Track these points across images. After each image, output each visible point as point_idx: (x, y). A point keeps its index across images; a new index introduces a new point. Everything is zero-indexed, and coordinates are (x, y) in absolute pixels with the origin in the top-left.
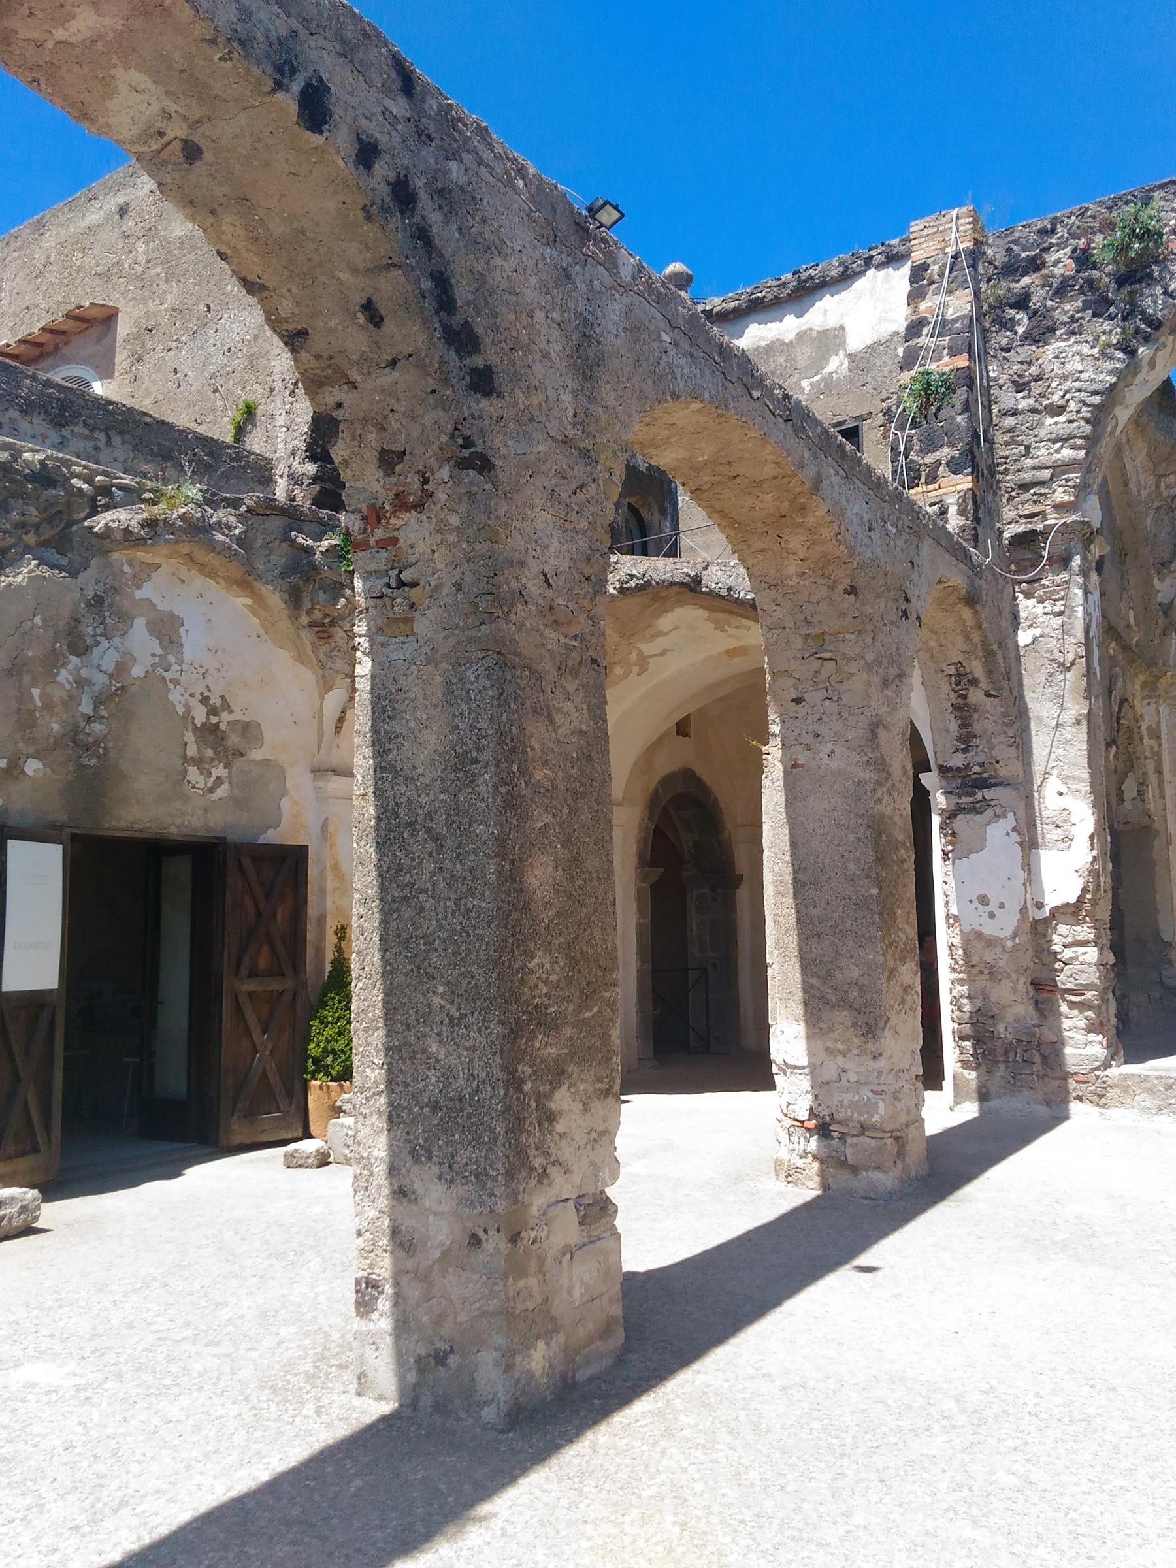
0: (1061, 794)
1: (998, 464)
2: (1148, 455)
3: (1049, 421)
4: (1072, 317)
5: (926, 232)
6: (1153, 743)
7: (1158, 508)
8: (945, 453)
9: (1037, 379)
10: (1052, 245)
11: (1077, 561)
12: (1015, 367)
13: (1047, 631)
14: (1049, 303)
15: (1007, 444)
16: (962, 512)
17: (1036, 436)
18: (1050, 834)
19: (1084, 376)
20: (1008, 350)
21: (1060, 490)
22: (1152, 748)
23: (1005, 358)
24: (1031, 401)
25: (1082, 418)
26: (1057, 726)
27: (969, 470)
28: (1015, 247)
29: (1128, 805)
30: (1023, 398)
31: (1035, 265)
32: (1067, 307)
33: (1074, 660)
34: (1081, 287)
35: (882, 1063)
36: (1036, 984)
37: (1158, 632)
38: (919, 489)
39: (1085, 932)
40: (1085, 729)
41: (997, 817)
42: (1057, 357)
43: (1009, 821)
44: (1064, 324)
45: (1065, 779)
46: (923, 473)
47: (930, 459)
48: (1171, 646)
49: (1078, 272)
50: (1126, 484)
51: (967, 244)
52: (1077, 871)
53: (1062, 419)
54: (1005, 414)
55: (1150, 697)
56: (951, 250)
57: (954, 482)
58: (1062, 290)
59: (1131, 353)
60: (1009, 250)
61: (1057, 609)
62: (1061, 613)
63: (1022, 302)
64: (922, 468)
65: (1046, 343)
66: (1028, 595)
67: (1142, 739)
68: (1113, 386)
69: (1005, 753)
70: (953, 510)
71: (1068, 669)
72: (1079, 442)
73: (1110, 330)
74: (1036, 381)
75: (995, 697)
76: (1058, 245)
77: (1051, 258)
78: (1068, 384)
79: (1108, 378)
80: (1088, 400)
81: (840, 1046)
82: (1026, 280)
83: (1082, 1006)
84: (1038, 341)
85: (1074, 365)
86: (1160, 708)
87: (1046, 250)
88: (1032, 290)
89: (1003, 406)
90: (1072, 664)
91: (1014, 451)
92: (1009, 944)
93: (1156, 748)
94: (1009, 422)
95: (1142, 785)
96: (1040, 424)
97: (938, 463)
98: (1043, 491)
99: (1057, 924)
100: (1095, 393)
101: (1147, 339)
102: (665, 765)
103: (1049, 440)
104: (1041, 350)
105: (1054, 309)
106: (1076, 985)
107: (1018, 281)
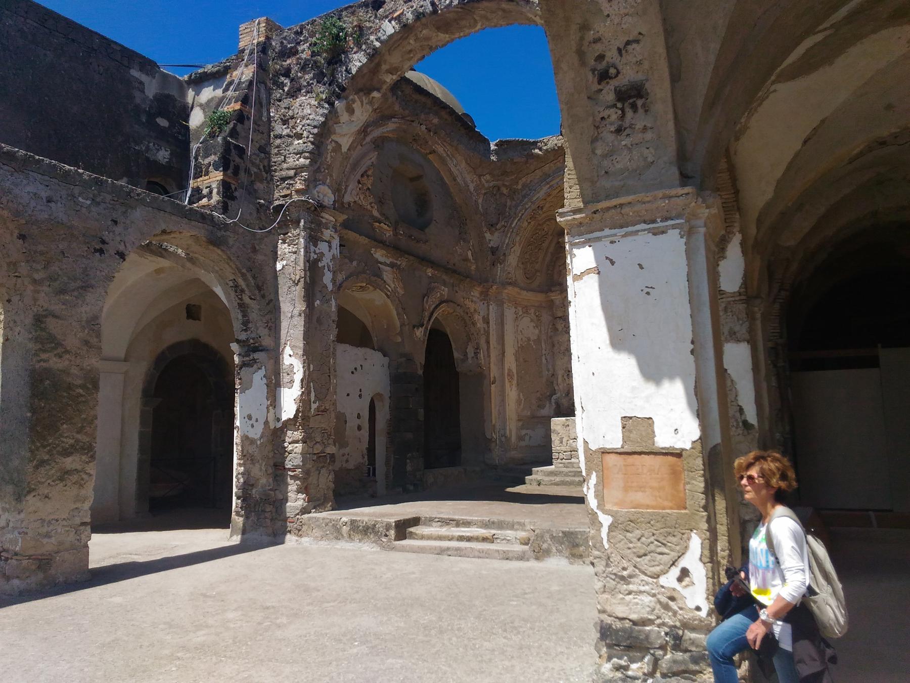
0: (290, 356)
1: (272, 166)
2: (466, 162)
3: (296, 142)
4: (308, 82)
5: (246, 31)
6: (485, 326)
7: (485, 194)
8: (213, 158)
9: (292, 118)
10: (301, 41)
11: (302, 223)
12: (282, 111)
13: (289, 262)
14: (299, 74)
15: (276, 154)
16: (218, 193)
17: (288, 151)
18: (285, 379)
19: (311, 117)
20: (280, 101)
21: (299, 182)
22: (484, 328)
23: (278, 105)
24: (288, 130)
25: (309, 141)
26: (292, 317)
27: (221, 169)
28: (284, 41)
29: (470, 361)
30: (285, 128)
31: (293, 52)
32: (307, 77)
33: (300, 279)
34: (312, 65)
35: (22, 515)
36: (275, 465)
37: (488, 263)
38: (201, 179)
39: (298, 435)
40: (303, 319)
41: (260, 369)
42: (300, 106)
43: (262, 372)
44: (305, 86)
45: (292, 347)
46: (204, 170)
47: (206, 161)
48: (497, 271)
49: (312, 57)
50: (455, 180)
51: (262, 39)
52: (295, 400)
53: (300, 141)
54: (276, 137)
55: (485, 300)
56: (255, 42)
57: (215, 175)
58: (303, 68)
59: (331, 104)
60: (282, 43)
61: (294, 250)
62: (295, 253)
63: (287, 73)
64: (203, 167)
65: (297, 98)
66: (284, 242)
67: (474, 324)
68: (324, 124)
69: (263, 332)
70: (215, 191)
71: (297, 284)
72: (307, 155)
73: (322, 90)
74: (292, 119)
75: (254, 299)
76: (304, 41)
77: (300, 48)
78: (304, 122)
79: (321, 119)
80: (312, 131)
81: (8, 506)
82: (288, 62)
83: (294, 478)
84: (293, 96)
85: (308, 111)
86: (491, 307)
87: (298, 44)
88: (292, 66)
89: (276, 133)
90: (299, 281)
91: (279, 159)
92: (259, 442)
93: (486, 329)
94: (278, 141)
95: (477, 348)
96: (291, 144)
97: (209, 164)
98: (291, 182)
99: (287, 431)
100: (315, 127)
101: (338, 97)
102: (171, 336)
103: (294, 153)
104: (295, 101)
105: (301, 78)
106: (292, 466)
107: (286, 61)
